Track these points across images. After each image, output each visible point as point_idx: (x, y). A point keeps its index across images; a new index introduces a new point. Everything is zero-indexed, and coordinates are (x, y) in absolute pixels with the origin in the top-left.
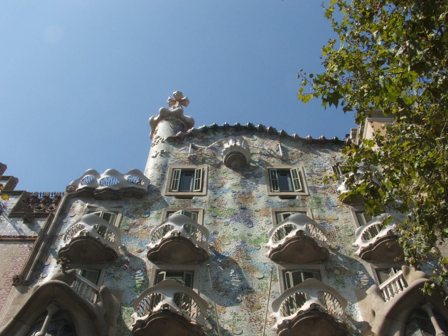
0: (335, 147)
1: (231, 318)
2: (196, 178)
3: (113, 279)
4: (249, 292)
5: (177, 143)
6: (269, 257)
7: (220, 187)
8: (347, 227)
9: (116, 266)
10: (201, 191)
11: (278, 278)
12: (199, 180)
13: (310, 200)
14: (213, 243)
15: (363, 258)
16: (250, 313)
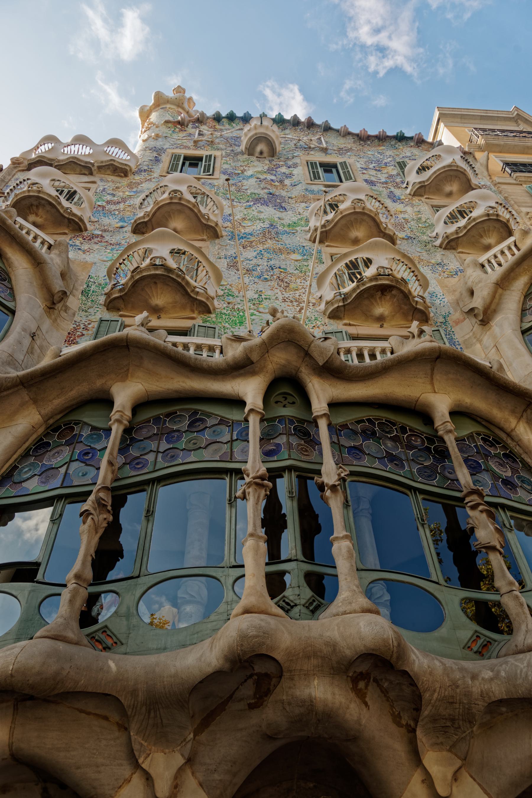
0: (399, 146)
1: (256, 296)
2: (206, 162)
3: (79, 251)
4: (281, 272)
5: (177, 129)
6: (310, 240)
7: (239, 174)
8: (420, 219)
9: (84, 239)
10: (213, 175)
11: (324, 260)
12: (209, 165)
14: (229, 223)
15: (445, 249)
16: (283, 293)
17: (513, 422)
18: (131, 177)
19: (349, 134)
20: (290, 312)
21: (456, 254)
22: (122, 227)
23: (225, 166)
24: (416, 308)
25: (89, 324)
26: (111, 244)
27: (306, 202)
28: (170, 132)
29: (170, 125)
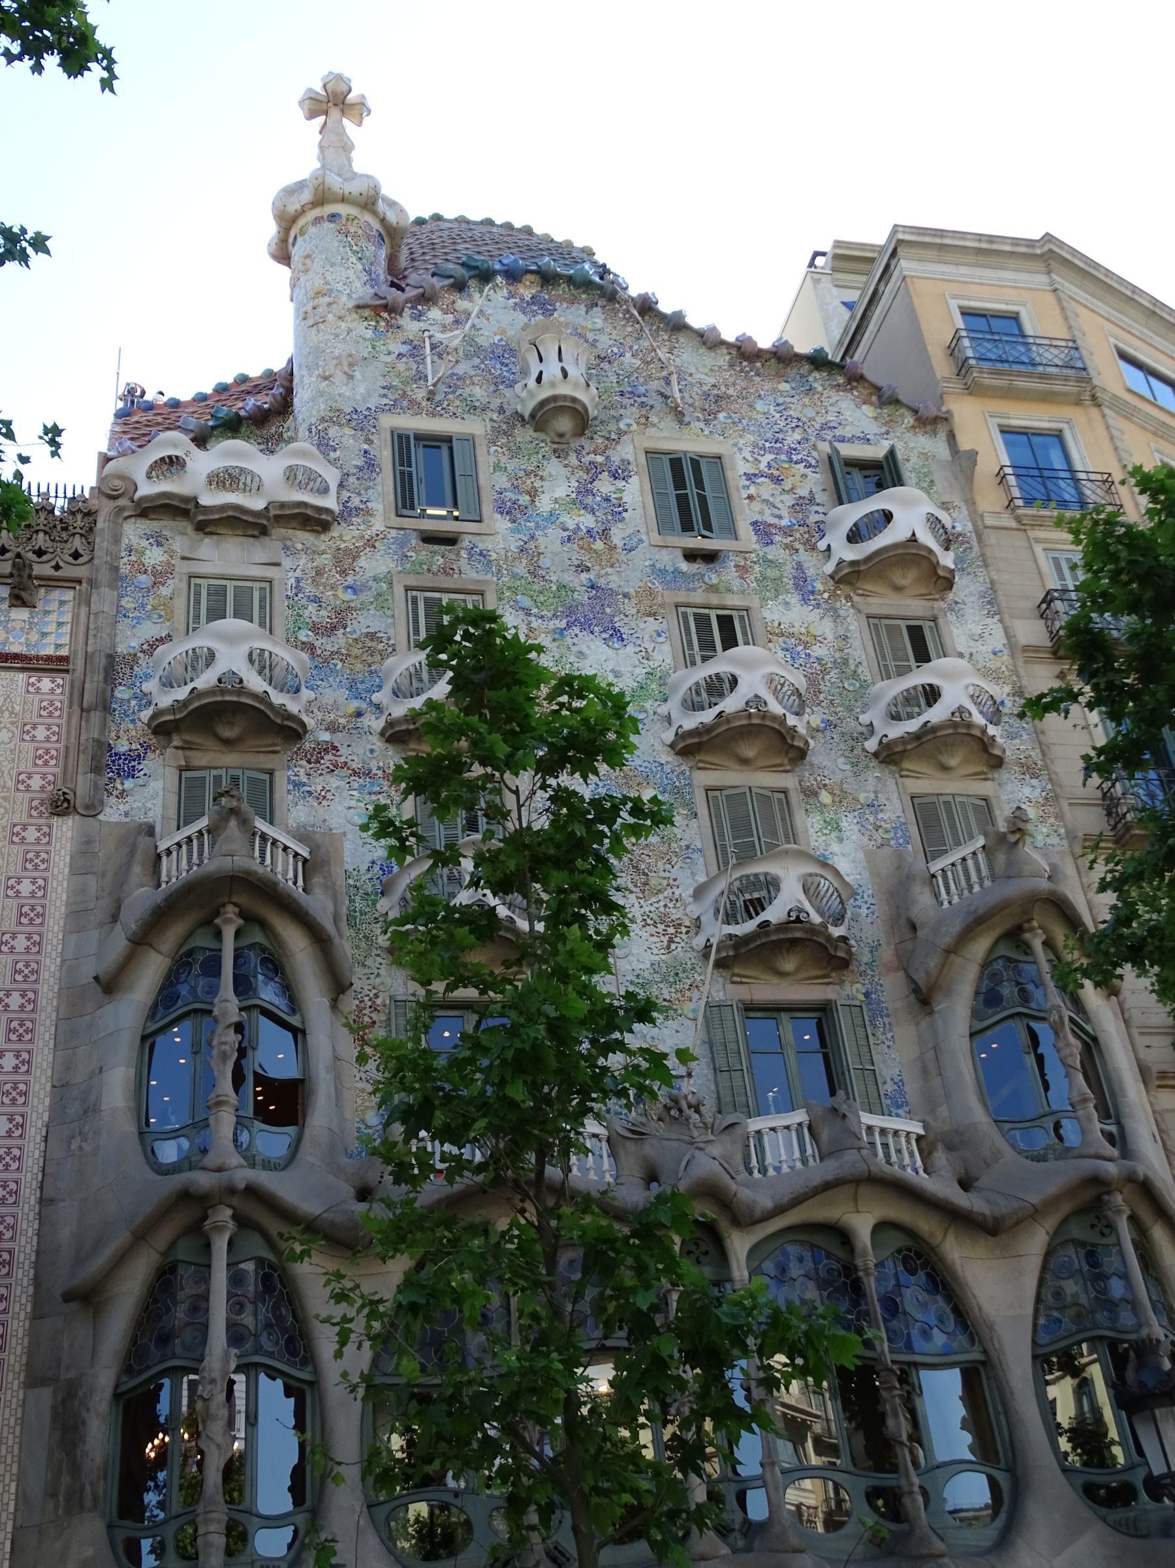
0: (816, 380)
8: (846, 662)
9: (309, 762)
13: (757, 568)
17: (939, 1235)
18: (336, 531)
19: (723, 343)
20: (655, 951)
21: (900, 780)
22: (359, 714)
23: (502, 481)
24: (835, 957)
25: (376, 996)
26: (355, 773)
27: (653, 615)
28: (369, 334)
29: (367, 313)
